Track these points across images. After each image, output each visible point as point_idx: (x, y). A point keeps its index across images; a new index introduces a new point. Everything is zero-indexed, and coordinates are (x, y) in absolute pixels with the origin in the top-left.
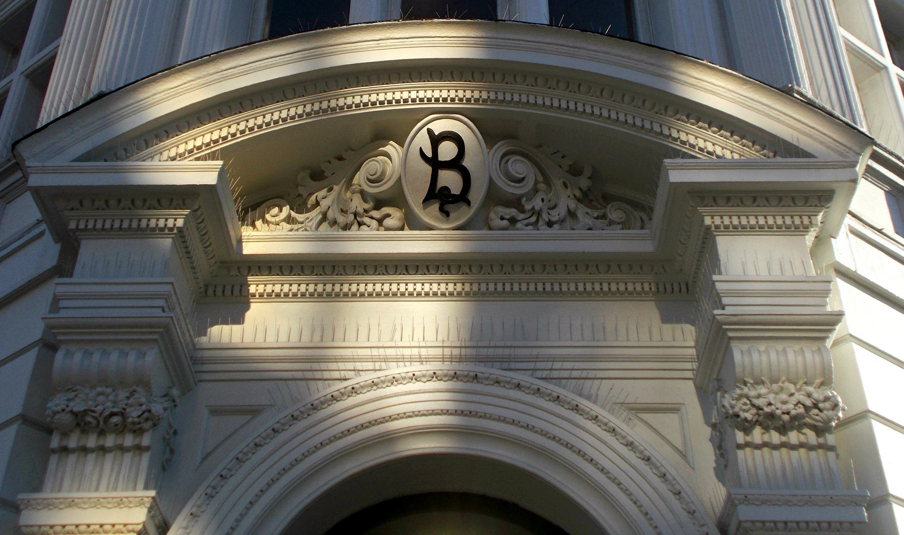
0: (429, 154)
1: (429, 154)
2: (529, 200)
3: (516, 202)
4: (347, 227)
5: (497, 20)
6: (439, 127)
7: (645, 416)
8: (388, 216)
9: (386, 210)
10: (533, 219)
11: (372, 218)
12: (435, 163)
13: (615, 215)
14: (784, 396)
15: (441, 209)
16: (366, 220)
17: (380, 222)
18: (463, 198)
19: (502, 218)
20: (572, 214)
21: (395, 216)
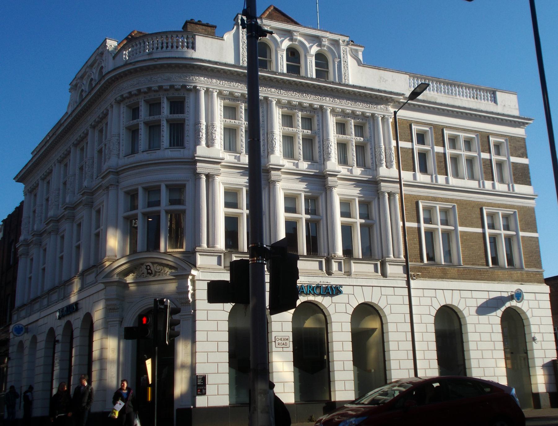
2: (161, 271)
3: (159, 272)
6: (147, 264)
12: (147, 269)
18: (152, 273)
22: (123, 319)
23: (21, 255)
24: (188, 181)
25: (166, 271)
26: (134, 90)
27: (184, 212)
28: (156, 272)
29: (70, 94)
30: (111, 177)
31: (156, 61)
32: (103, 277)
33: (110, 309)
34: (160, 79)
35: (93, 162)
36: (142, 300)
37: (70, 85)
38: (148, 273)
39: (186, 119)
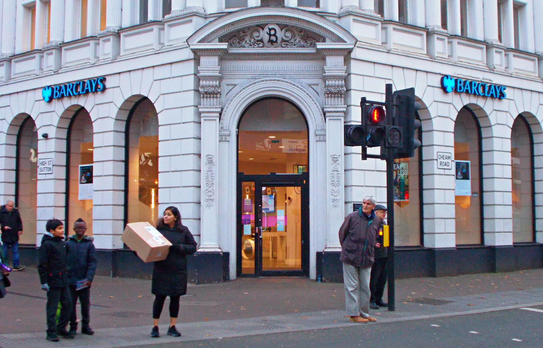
0: (269, 33)
1: (269, 33)
3: (287, 41)
4: (251, 45)
5: (284, 7)
6: (271, 27)
7: (313, 86)
8: (260, 44)
9: (259, 43)
10: (291, 44)
11: (256, 44)
12: (270, 35)
14: (335, 89)
15: (271, 44)
16: (255, 44)
17: (258, 45)
18: (276, 41)
19: (284, 45)
20: (299, 41)
21: (261, 45)
22: (222, 110)
25: (297, 41)
28: (283, 41)
33: (206, 93)
36: (255, 83)
38: (271, 41)
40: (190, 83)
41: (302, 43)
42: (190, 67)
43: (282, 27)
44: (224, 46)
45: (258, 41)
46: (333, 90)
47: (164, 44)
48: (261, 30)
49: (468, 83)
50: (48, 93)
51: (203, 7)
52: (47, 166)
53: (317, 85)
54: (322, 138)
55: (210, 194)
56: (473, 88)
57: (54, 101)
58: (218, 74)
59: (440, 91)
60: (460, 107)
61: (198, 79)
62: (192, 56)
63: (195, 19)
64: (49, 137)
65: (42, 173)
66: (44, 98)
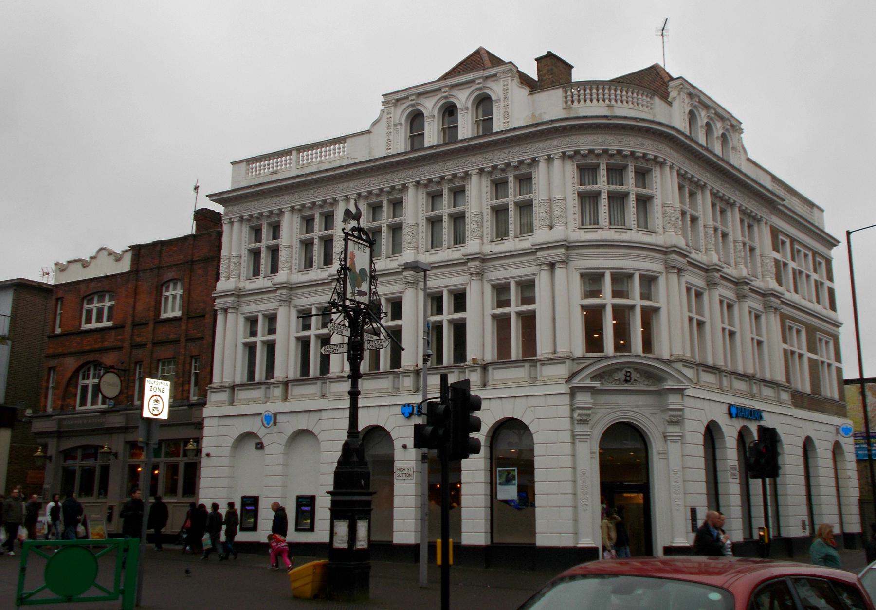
3: (636, 380)
6: (628, 370)
12: (626, 376)
13: (651, 381)
18: (629, 381)
23: (225, 310)
24: (661, 273)
26: (598, 149)
27: (656, 310)
28: (635, 380)
29: (383, 108)
30: (562, 251)
31: (638, 122)
32: (579, 379)
33: (581, 420)
34: (632, 142)
35: (482, 219)
37: (383, 95)
38: (626, 381)
39: (655, 197)
40: (566, 411)
41: (646, 383)
42: (566, 399)
43: (635, 369)
44: (597, 385)
45: (616, 380)
46: (674, 419)
47: (536, 378)
48: (619, 372)
49: (743, 410)
50: (408, 410)
51: (570, 349)
52: (406, 472)
53: (655, 414)
54: (665, 454)
55: (585, 500)
56: (746, 413)
57: (413, 417)
58: (591, 406)
59: (727, 416)
60: (739, 428)
61: (573, 410)
62: (568, 391)
63: (567, 361)
64: (408, 447)
65: (399, 478)
66: (403, 414)
